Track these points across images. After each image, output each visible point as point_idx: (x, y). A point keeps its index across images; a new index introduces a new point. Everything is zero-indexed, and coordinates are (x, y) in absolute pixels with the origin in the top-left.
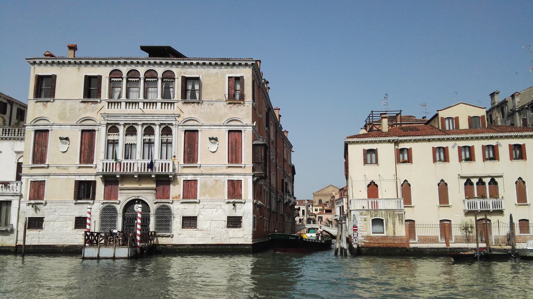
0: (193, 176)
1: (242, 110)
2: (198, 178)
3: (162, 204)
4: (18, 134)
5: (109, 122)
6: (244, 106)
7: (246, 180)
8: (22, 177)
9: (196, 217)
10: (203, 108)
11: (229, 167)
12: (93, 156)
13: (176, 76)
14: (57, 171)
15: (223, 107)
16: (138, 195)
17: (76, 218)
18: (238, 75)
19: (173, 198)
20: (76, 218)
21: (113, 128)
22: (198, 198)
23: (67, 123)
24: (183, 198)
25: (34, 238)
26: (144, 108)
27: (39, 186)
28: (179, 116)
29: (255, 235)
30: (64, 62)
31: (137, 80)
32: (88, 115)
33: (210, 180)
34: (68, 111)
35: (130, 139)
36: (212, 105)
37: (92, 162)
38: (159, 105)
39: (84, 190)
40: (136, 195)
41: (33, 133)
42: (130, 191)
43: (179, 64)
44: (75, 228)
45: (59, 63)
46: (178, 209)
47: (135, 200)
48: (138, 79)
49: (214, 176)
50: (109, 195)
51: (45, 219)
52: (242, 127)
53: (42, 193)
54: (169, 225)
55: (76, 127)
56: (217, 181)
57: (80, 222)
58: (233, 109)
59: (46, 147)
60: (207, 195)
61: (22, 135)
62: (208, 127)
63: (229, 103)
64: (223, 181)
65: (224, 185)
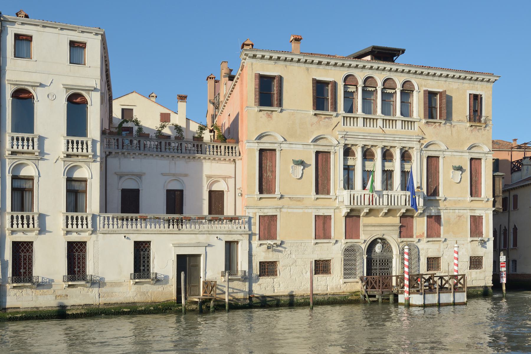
7: (487, 215)
19: (417, 237)
40: (379, 233)
47: (376, 239)
49: (457, 211)
56: (460, 216)
57: (322, 267)
65: (467, 221)
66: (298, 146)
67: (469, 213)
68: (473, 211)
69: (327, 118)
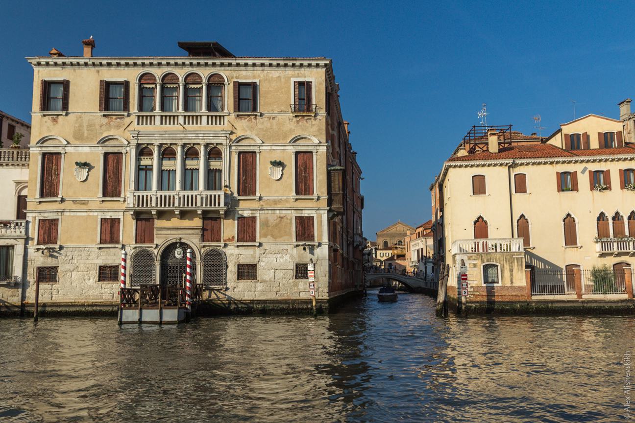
0: (250, 212)
1: (314, 125)
4: (18, 158)
6: (315, 120)
7: (320, 216)
8: (28, 215)
9: (256, 265)
10: (262, 123)
11: (297, 200)
12: (121, 187)
13: (226, 81)
15: (288, 122)
16: (180, 236)
17: (100, 267)
19: (224, 241)
20: (100, 267)
21: (143, 151)
22: (258, 240)
24: (238, 241)
25: (50, 294)
26: (185, 124)
27: (50, 226)
28: (232, 133)
29: (332, 288)
32: (112, 133)
34: (85, 128)
35: (167, 164)
36: (274, 118)
37: (119, 195)
39: (110, 231)
41: (40, 158)
42: (169, 232)
43: (230, 65)
44: (99, 280)
45: (72, 64)
46: (232, 255)
47: (176, 243)
48: (177, 85)
49: (278, 212)
50: (144, 235)
51: (60, 269)
52: (313, 147)
53: (54, 234)
54: (221, 275)
55: (97, 148)
56: (282, 218)
57: (107, 273)
58: (300, 123)
59: (58, 175)
60: (269, 237)
61: (27, 159)
63: (296, 116)
64: (289, 218)
65: (291, 223)
66: (84, 148)
67: (294, 214)
68: (300, 211)
69: (119, 118)
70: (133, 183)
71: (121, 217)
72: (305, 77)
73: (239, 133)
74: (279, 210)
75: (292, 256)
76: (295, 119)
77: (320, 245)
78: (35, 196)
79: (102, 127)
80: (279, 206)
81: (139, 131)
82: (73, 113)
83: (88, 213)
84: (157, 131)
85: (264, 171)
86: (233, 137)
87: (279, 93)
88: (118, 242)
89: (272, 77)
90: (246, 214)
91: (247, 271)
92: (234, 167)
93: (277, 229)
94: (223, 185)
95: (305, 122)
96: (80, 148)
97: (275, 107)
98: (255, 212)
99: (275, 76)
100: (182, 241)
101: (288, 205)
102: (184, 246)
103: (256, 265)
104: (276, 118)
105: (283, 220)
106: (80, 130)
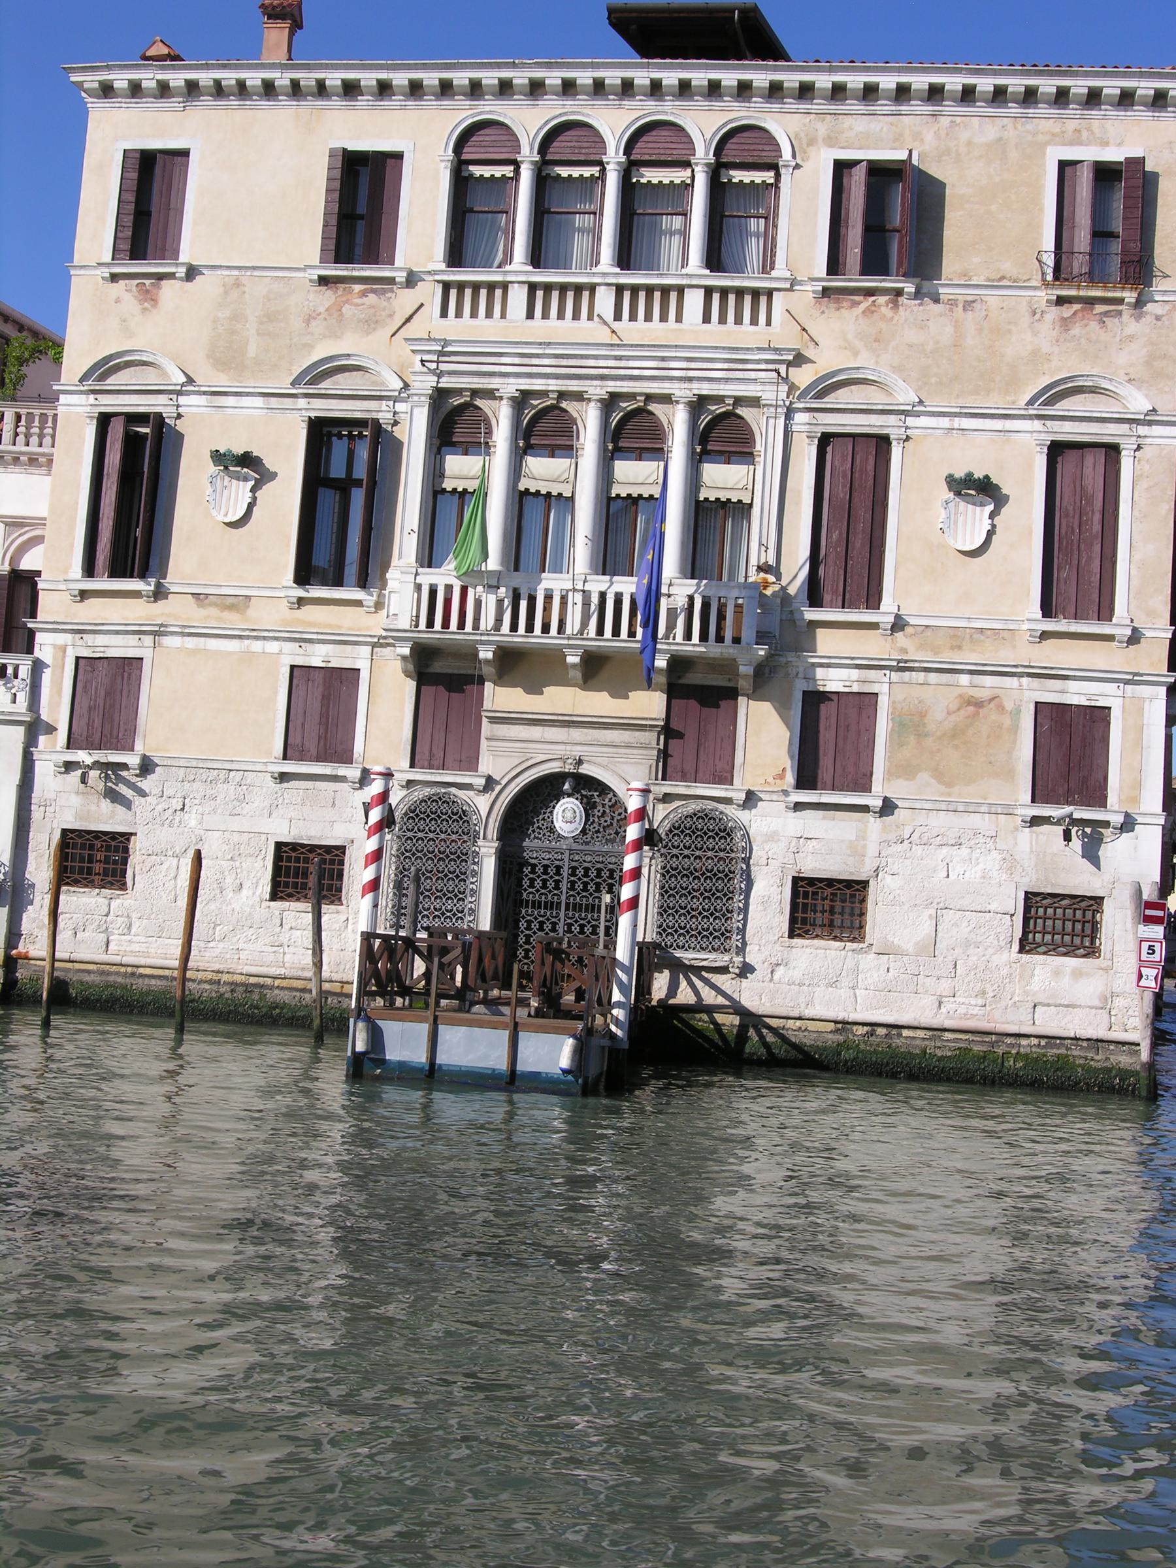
0: (855, 674)
2: (881, 684)
3: (693, 807)
5: (446, 382)
6: (1138, 318)
7: (1137, 709)
8: (40, 638)
9: (864, 884)
11: (1045, 635)
14: (198, 616)
15: (1026, 319)
16: (577, 751)
17: (279, 846)
18: (1114, 154)
20: (279, 846)
23: (250, 385)
26: (618, 317)
28: (800, 359)
30: (241, 85)
31: (587, 172)
33: (939, 697)
38: (694, 301)
40: (560, 750)
42: (536, 732)
44: (274, 896)
45: (219, 90)
46: (773, 837)
47: (560, 777)
48: (595, 171)
49: (964, 679)
55: (288, 403)
56: (978, 704)
57: (305, 873)
58: (1076, 330)
60: (924, 777)
61: (47, 440)
62: (945, 422)
63: (1061, 301)
64: (1009, 706)
65: (1015, 729)
67: (1027, 695)
68: (1058, 684)
70: (415, 536)
71: (363, 665)
72: (1107, 144)
73: (827, 359)
74: (971, 672)
75: (1010, 863)
76: (1054, 312)
77: (1128, 825)
78: (66, 571)
79: (313, 324)
80: (971, 657)
81: (446, 343)
82: (213, 268)
83: (247, 642)
84: (515, 340)
85: (918, 516)
86: (803, 377)
87: (994, 208)
88: (346, 757)
89: (969, 143)
90: (833, 680)
91: (828, 906)
92: (800, 492)
93: (956, 747)
94: (754, 561)
95: (1094, 325)
96: (230, 401)
97: (976, 260)
98: (872, 674)
99: (981, 139)
100: (585, 769)
101: (1006, 656)
102: (589, 789)
103: (864, 884)
104: (977, 306)
105: (982, 712)
106: (233, 332)
